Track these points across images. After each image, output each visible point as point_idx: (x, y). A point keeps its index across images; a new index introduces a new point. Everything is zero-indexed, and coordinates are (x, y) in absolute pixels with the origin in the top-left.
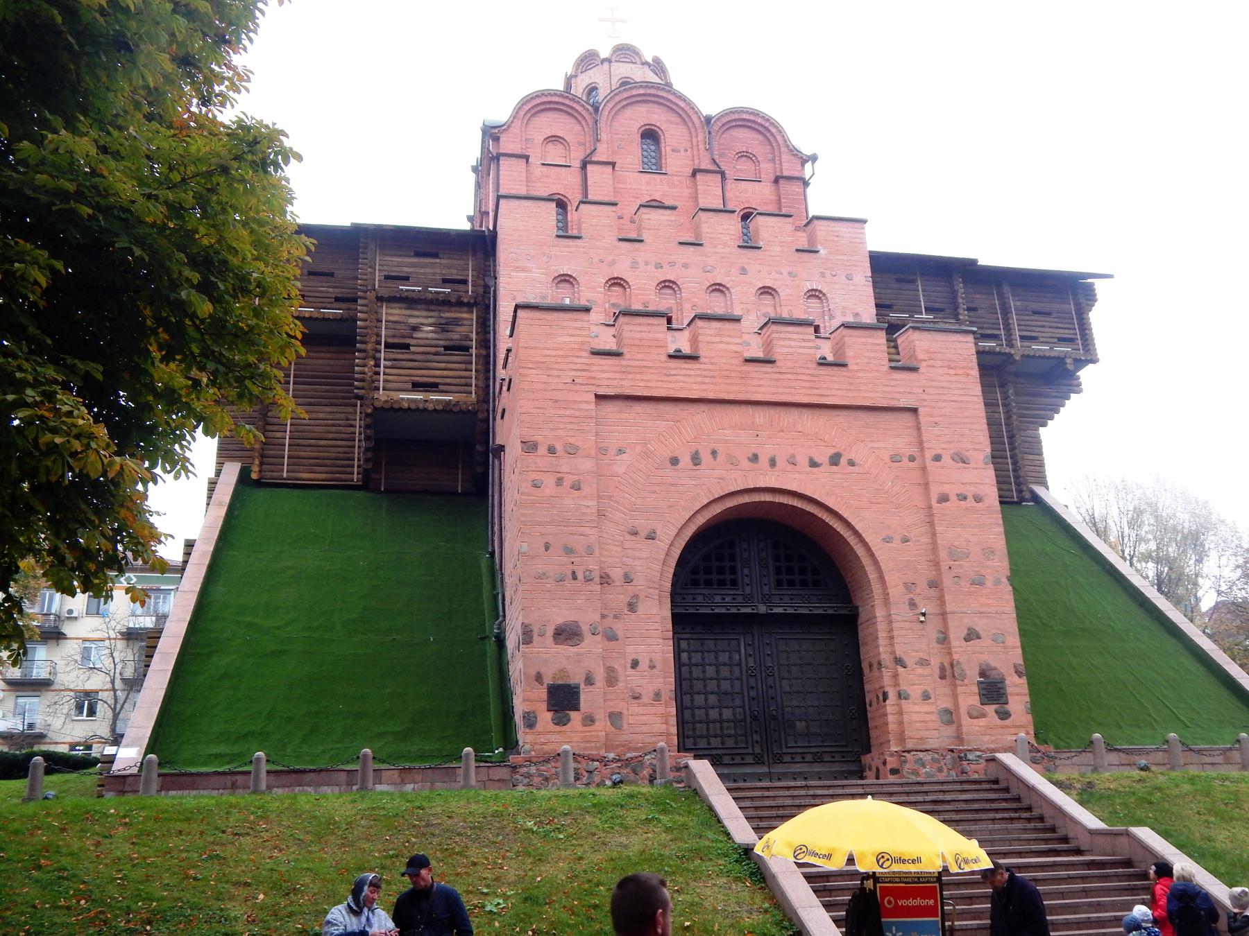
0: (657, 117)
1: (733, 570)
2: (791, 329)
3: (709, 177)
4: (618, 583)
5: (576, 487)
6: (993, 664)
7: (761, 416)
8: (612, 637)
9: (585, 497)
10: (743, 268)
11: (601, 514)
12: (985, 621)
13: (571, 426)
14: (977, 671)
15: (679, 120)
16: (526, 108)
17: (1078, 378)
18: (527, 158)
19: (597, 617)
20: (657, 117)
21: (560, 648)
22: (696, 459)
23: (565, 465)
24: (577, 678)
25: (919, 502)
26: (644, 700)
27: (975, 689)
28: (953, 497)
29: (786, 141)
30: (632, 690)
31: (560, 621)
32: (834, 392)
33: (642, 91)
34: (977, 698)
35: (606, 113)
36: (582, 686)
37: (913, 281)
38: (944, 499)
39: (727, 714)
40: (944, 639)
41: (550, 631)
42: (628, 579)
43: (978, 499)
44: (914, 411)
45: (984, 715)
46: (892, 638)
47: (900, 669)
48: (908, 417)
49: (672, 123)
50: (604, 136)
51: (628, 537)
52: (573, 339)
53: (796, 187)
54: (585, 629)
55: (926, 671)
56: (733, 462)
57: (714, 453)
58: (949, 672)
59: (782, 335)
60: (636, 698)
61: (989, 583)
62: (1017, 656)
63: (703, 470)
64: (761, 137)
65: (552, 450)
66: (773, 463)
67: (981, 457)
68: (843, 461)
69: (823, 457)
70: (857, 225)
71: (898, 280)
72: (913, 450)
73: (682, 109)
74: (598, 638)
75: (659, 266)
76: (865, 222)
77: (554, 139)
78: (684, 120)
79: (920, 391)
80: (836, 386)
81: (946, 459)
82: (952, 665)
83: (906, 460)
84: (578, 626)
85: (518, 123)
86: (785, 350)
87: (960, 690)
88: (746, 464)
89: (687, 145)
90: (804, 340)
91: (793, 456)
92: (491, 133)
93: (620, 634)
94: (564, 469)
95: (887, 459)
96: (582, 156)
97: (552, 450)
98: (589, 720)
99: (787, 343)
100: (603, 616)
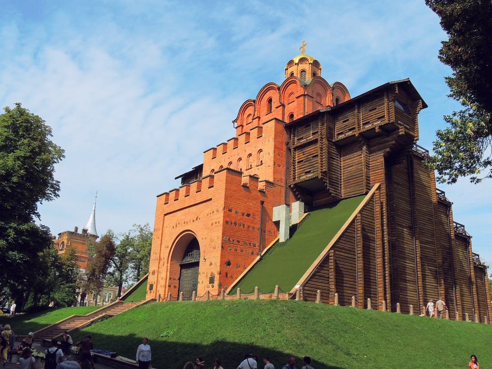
24: (153, 283)
28: (214, 223)
31: (153, 270)
37: (310, 125)
38: (212, 224)
49: (274, 93)
61: (217, 248)
62: (218, 269)
63: (177, 229)
69: (195, 219)
71: (305, 127)
77: (250, 115)
81: (215, 212)
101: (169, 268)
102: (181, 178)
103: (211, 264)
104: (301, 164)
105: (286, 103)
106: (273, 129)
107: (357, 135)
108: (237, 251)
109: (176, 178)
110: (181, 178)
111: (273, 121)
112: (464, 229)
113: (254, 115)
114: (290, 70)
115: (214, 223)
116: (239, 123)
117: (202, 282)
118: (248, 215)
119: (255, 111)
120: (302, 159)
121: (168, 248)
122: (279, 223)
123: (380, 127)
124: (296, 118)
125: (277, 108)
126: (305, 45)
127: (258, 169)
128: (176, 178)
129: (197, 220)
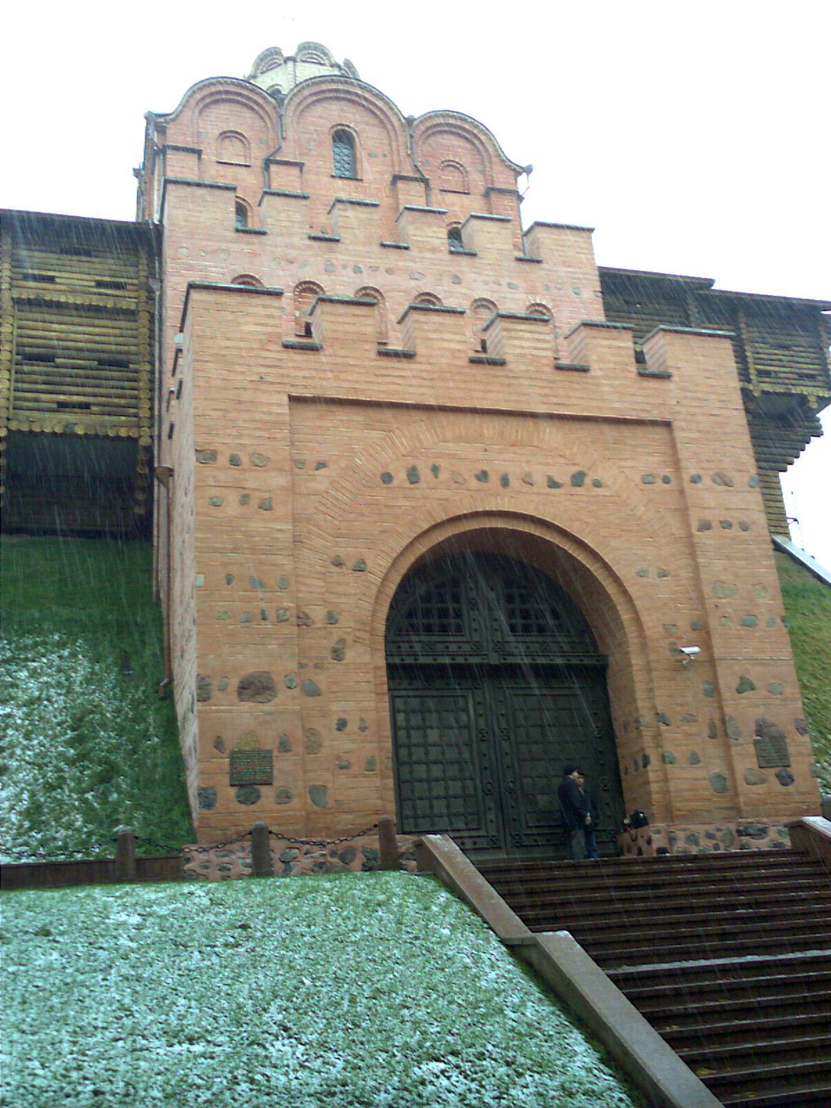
0: (352, 118)
1: (458, 615)
2: (523, 327)
3: (414, 185)
4: (319, 625)
5: (266, 506)
6: (770, 719)
7: (490, 427)
8: (313, 692)
9: (277, 519)
10: (456, 277)
11: (297, 541)
12: (759, 669)
13: (258, 433)
14: (753, 727)
15: (375, 121)
16: (198, 96)
17: (818, 420)
18: (199, 153)
19: (292, 665)
20: (352, 118)
21: (247, 706)
22: (413, 476)
23: (252, 481)
24: (269, 742)
25: (679, 532)
26: (355, 769)
29: (498, 152)
30: (338, 758)
32: (575, 401)
34: (755, 760)
35: (292, 108)
36: (275, 753)
38: (706, 526)
39: (455, 787)
40: (714, 691)
41: (234, 682)
42: (332, 619)
43: (744, 527)
44: (668, 424)
45: (763, 781)
46: (651, 690)
47: (663, 727)
48: (660, 433)
49: (367, 124)
50: (290, 134)
51: (334, 569)
52: (258, 329)
53: (507, 201)
54: (279, 682)
55: (693, 729)
56: (457, 481)
57: (435, 470)
58: (721, 730)
59: (513, 334)
60: (341, 768)
61: (762, 624)
64: (468, 145)
65: (234, 461)
66: (505, 482)
67: (746, 479)
68: (588, 481)
69: (563, 477)
70: (584, 234)
72: (667, 471)
73: (381, 109)
74: (296, 692)
75: (357, 270)
76: (591, 230)
78: (381, 122)
79: (673, 402)
80: (578, 394)
81: (707, 481)
82: (723, 721)
83: (659, 481)
84: (271, 678)
85: (187, 114)
86: (518, 351)
87: (734, 750)
88: (474, 483)
89: (386, 149)
90: (538, 340)
91: (529, 475)
92: (157, 124)
93: (323, 687)
94: (249, 485)
95: (637, 479)
96: (264, 154)
97: (234, 461)
98: (284, 796)
99: (517, 342)
100: (301, 666)
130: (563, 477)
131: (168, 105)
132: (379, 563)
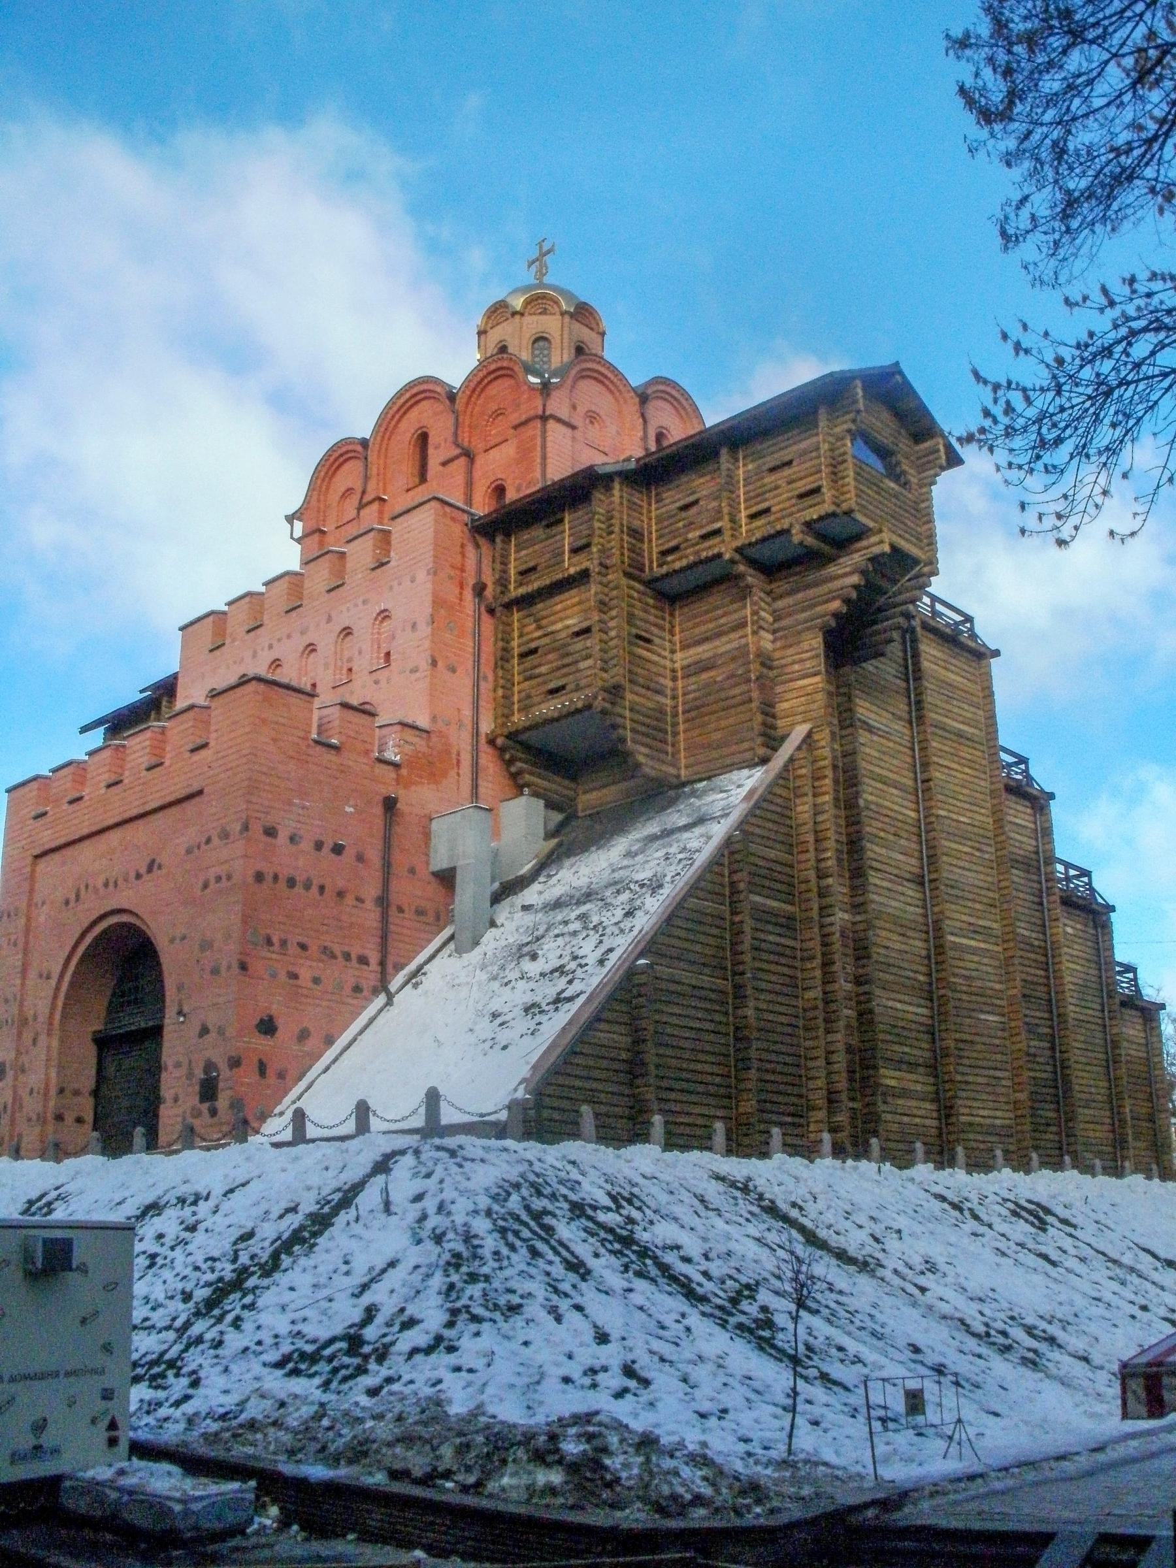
27: (197, 1088)
33: (408, 395)
37: (561, 521)
49: (436, 414)
57: (87, 887)
69: (143, 870)
71: (548, 526)
77: (350, 490)
81: (216, 841)
88: (102, 890)
101: (55, 1054)
102: (102, 729)
103: (205, 1031)
104: (532, 660)
105: (478, 445)
106: (430, 534)
107: (727, 556)
108: (299, 982)
109: (85, 729)
110: (102, 729)
111: (427, 506)
112: (1090, 883)
113: (364, 492)
114: (495, 336)
115: (212, 880)
116: (314, 521)
117: (176, 1100)
118: (338, 850)
119: (366, 478)
120: (533, 645)
121: (48, 977)
122: (454, 877)
123: (808, 524)
124: (511, 495)
125: (444, 464)
126: (548, 252)
127: (376, 682)
128: (85, 729)
129: (150, 869)
130: (143, 870)
131: (295, 502)
132: (56, 969)
